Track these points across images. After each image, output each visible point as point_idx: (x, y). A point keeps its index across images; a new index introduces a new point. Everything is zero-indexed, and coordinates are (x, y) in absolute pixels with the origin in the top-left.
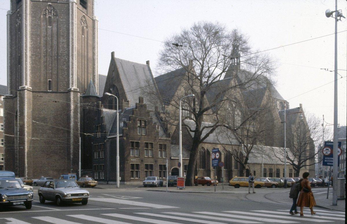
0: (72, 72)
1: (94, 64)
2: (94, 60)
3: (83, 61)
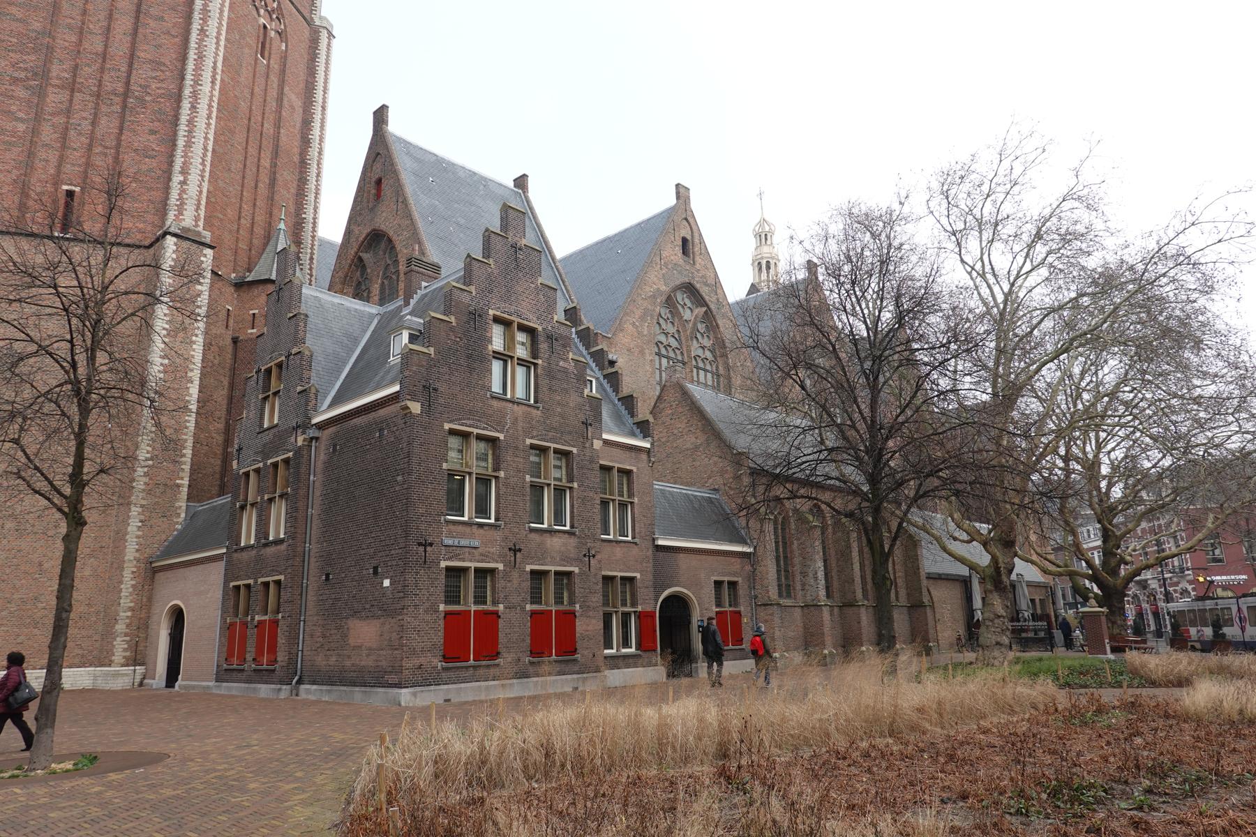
0: (184, 163)
1: (302, 181)
2: (303, 165)
3: (252, 151)
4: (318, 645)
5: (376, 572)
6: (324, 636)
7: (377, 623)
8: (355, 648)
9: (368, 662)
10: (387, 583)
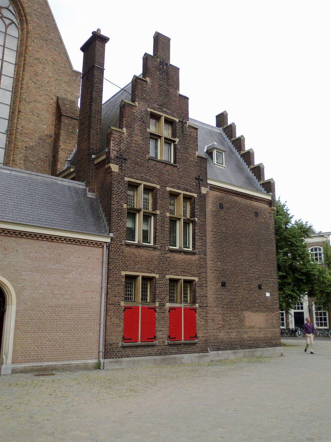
4: (220, 326)
5: (260, 287)
6: (224, 320)
7: (264, 314)
8: (250, 327)
9: (261, 335)
10: (268, 294)
